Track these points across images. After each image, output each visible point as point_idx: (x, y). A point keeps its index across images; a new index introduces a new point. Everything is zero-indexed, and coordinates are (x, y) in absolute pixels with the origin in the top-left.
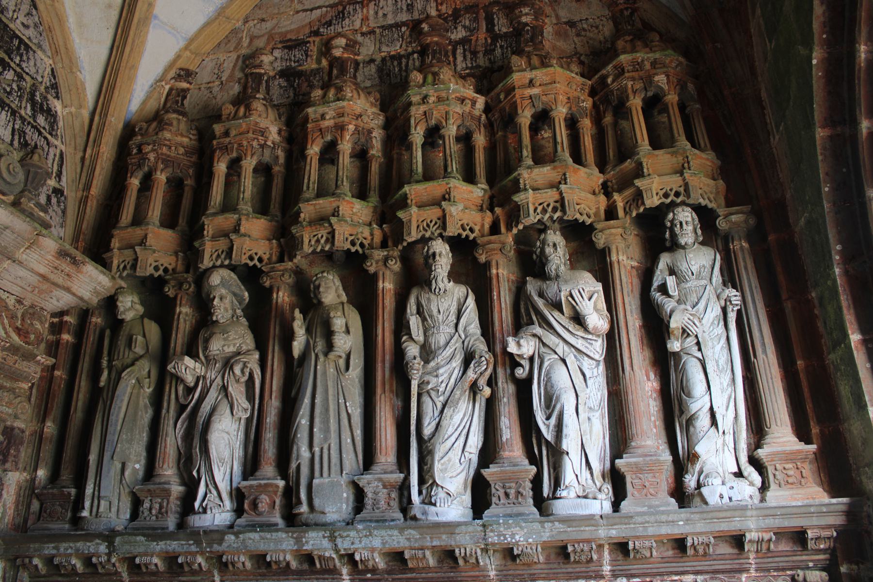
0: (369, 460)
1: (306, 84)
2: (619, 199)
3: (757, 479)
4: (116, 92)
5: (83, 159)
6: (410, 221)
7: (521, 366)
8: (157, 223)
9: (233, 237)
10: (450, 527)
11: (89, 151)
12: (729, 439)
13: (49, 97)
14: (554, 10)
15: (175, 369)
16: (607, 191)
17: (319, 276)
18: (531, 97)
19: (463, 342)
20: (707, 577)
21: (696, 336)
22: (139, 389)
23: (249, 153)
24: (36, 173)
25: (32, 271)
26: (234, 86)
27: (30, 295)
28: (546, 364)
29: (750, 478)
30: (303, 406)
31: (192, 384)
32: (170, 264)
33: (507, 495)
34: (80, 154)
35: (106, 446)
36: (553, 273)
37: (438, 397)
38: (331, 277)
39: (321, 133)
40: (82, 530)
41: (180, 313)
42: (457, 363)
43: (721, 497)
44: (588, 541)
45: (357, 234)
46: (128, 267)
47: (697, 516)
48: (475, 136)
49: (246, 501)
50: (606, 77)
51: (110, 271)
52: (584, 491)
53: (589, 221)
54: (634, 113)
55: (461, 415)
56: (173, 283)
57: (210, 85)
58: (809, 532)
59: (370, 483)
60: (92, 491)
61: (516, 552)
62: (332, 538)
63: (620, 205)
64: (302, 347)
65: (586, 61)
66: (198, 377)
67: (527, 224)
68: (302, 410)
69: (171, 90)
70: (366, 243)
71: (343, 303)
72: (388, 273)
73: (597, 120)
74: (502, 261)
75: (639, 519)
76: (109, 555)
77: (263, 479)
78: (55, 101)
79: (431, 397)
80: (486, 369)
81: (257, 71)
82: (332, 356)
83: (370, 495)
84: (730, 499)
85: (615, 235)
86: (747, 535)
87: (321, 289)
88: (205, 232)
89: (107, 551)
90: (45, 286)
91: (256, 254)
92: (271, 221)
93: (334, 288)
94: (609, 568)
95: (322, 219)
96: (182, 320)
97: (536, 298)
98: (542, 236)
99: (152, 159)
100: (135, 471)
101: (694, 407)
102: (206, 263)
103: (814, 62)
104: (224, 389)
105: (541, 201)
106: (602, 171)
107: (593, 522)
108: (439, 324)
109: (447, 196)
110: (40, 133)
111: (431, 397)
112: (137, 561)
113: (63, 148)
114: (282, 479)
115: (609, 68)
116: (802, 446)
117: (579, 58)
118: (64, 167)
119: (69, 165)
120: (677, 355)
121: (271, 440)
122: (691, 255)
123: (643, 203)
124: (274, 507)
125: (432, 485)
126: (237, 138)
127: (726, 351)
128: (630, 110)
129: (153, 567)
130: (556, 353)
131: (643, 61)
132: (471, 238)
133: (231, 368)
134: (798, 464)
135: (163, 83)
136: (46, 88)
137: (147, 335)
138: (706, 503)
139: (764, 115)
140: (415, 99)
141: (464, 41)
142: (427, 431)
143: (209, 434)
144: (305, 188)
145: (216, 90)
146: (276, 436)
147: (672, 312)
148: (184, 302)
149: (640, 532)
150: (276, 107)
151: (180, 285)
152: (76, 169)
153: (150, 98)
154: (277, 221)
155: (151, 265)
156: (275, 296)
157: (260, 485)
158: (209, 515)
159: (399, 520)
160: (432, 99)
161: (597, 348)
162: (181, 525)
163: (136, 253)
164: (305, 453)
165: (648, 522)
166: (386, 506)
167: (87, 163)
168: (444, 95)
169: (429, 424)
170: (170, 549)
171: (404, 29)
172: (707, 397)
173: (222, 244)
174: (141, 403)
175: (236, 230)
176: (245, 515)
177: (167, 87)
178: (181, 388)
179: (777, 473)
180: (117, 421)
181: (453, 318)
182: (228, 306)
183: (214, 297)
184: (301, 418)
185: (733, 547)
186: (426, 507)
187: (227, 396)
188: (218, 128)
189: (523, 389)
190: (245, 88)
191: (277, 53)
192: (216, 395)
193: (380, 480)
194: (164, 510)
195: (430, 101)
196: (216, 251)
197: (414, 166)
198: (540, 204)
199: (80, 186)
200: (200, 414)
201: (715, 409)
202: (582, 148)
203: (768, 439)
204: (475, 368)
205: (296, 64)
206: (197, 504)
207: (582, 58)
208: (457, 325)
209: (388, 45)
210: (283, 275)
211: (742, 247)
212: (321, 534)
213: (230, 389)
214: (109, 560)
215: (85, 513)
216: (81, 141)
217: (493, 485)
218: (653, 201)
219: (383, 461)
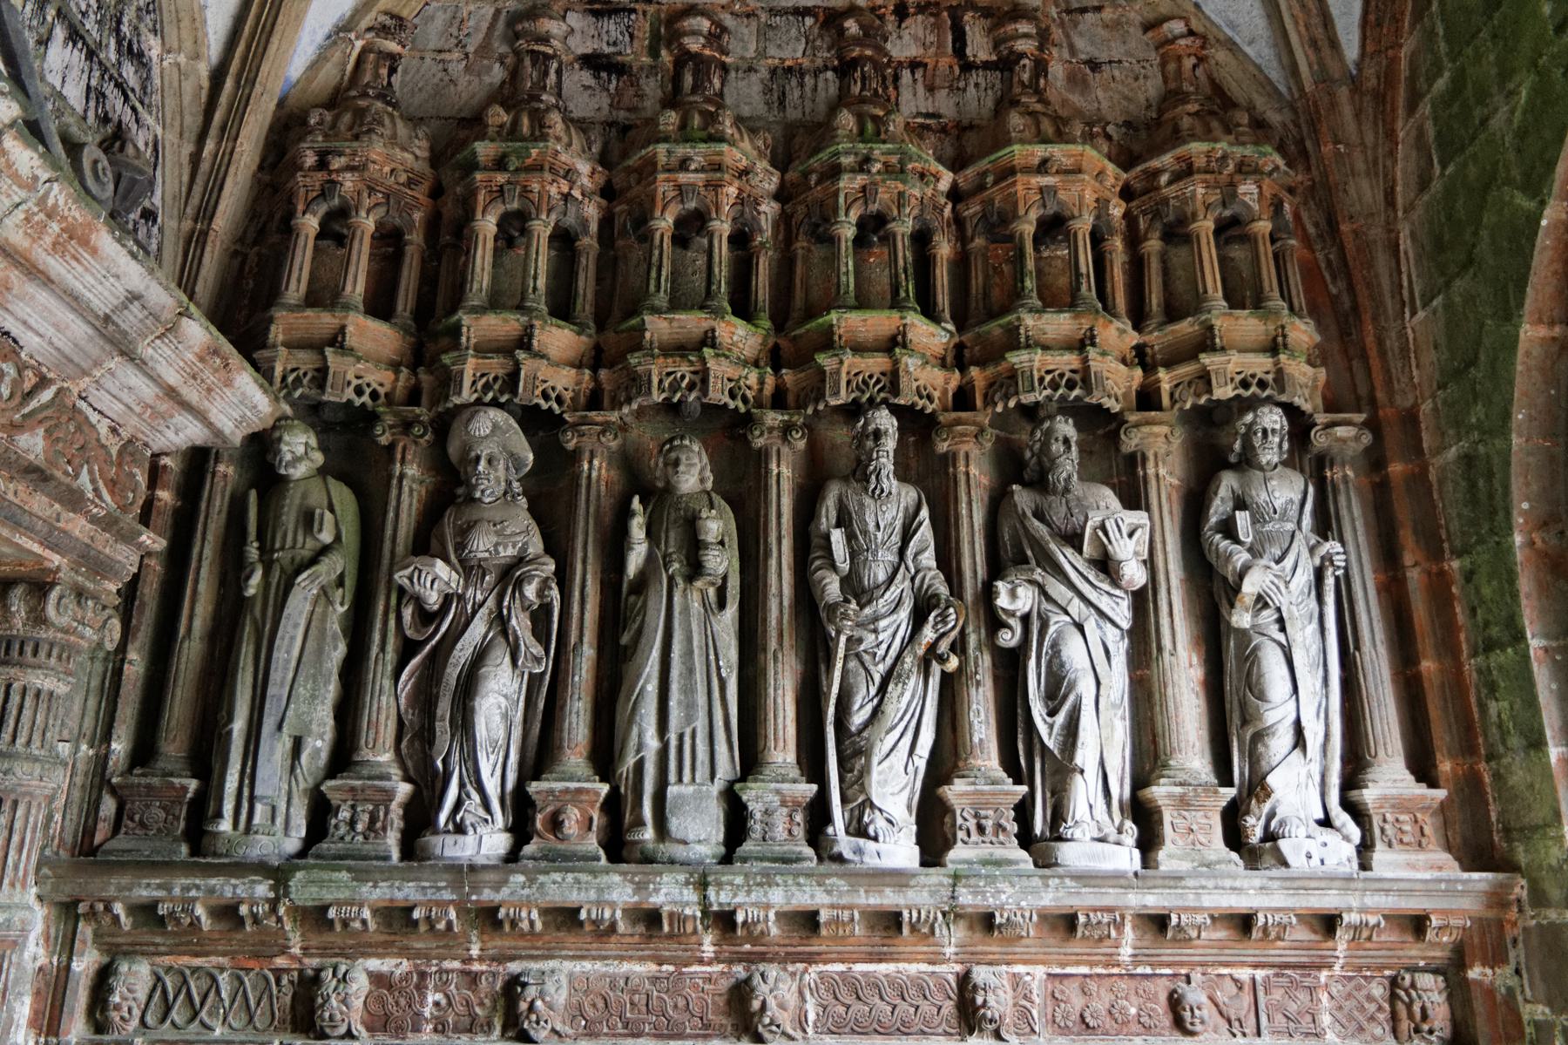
0: (751, 761)
1: (631, 91)
2: (1165, 379)
3: (1355, 833)
4: (275, 40)
5: (195, 159)
6: (838, 372)
7: (1010, 627)
8: (361, 307)
9: (521, 355)
10: (898, 878)
11: (210, 146)
12: (1316, 769)
13: (142, 26)
14: (1068, 36)
15: (411, 579)
16: (1142, 357)
18: (1041, 190)
19: (913, 579)
20: (1271, 972)
21: (1279, 610)
22: (326, 607)
23: (545, 207)
24: (133, 182)
25: (155, 379)
26: (490, 68)
27: (134, 421)
28: (1052, 629)
29: (1344, 831)
31: (436, 607)
32: (381, 385)
33: (981, 829)
34: (188, 148)
35: (267, 706)
36: (1060, 487)
37: (876, 665)
38: (696, 448)
39: (681, 194)
40: (215, 855)
41: (402, 476)
42: (904, 614)
43: (1309, 857)
44: (1110, 910)
45: (738, 381)
46: (305, 381)
47: (1276, 884)
48: (936, 238)
49: (539, 817)
50: (1157, 173)
51: (271, 383)
52: (1100, 829)
53: (1115, 407)
54: (1204, 241)
55: (907, 695)
56: (389, 420)
57: (443, 56)
58: (1433, 917)
59: (756, 796)
60: (236, 784)
61: (998, 920)
62: (702, 885)
63: (1166, 387)
65: (1115, 137)
66: (447, 596)
67: (1024, 401)
69: (365, 51)
70: (749, 394)
71: (708, 493)
72: (785, 450)
73: (1133, 240)
74: (975, 452)
75: (1190, 883)
76: (274, 904)
77: (571, 779)
78: (151, 36)
79: (863, 664)
80: (954, 628)
81: (542, 48)
82: (699, 584)
83: (758, 816)
84: (1322, 862)
85: (1157, 435)
86: (1345, 916)
87: (682, 468)
88: (464, 339)
89: (272, 895)
90: (164, 406)
91: (553, 389)
92: (579, 334)
94: (1130, 951)
95: (679, 349)
96: (406, 489)
97: (1037, 523)
98: (1047, 425)
99: (348, 184)
100: (317, 751)
101: (1270, 717)
102: (467, 395)
103: (1544, 223)
104: (500, 621)
105: (1051, 367)
106: (1138, 326)
107: (1122, 882)
109: (900, 338)
110: (126, 99)
111: (863, 664)
112: (332, 913)
113: (159, 131)
114: (602, 780)
115: (1167, 159)
116: (1421, 790)
117: (1104, 129)
118: (159, 168)
119: (168, 164)
120: (1243, 636)
122: (1274, 483)
123: (1210, 391)
124: (590, 829)
125: (862, 807)
126: (522, 176)
127: (1318, 636)
128: (1198, 237)
129: (357, 925)
130: (1067, 613)
131: (1224, 157)
132: (929, 411)
133: (519, 584)
134: (1419, 816)
135: (352, 36)
136: (139, 9)
137: (337, 508)
138: (1284, 863)
139: (1400, 273)
140: (846, 161)
141: (914, 65)
142: (858, 719)
143: (478, 699)
144: (652, 288)
145: (457, 68)
146: (589, 706)
147: (1246, 569)
148: (409, 457)
149: (1191, 901)
150: (582, 125)
151: (406, 426)
152: (180, 176)
153: (326, 59)
154: (590, 336)
155: (349, 383)
156: (586, 466)
157: (567, 791)
158: (470, 839)
160: (877, 167)
161: (1122, 612)
162: (411, 848)
163: (325, 359)
164: (652, 743)
165: (1203, 887)
166: (785, 835)
167: (205, 166)
168: (894, 159)
169: (862, 707)
170: (399, 895)
171: (809, 21)
172: (1292, 703)
173: (497, 366)
174: (329, 633)
175: (524, 341)
176: (535, 839)
177: (359, 44)
178: (408, 613)
179: (1387, 827)
180: (288, 661)
181: (896, 539)
182: (501, 473)
183: (478, 458)
184: (646, 682)
185: (1315, 932)
186: (861, 841)
187: (504, 632)
188: (484, 150)
189: (1010, 667)
190: (515, 74)
191: (574, 19)
192: (483, 630)
193: (778, 792)
194: (379, 825)
195: (874, 170)
196: (483, 375)
197: (843, 279)
198: (1048, 372)
199: (189, 210)
200: (452, 660)
201: (1304, 723)
202: (1109, 285)
203: (1372, 774)
204: (936, 624)
205: (612, 49)
206: (443, 817)
207: (1110, 129)
208: (902, 552)
209: (779, 46)
210: (603, 432)
211: (1345, 476)
212: (682, 878)
213: (514, 622)
214: (274, 910)
215: (225, 826)
216: (193, 121)
217: (958, 812)
218: (1224, 392)
219: (780, 760)
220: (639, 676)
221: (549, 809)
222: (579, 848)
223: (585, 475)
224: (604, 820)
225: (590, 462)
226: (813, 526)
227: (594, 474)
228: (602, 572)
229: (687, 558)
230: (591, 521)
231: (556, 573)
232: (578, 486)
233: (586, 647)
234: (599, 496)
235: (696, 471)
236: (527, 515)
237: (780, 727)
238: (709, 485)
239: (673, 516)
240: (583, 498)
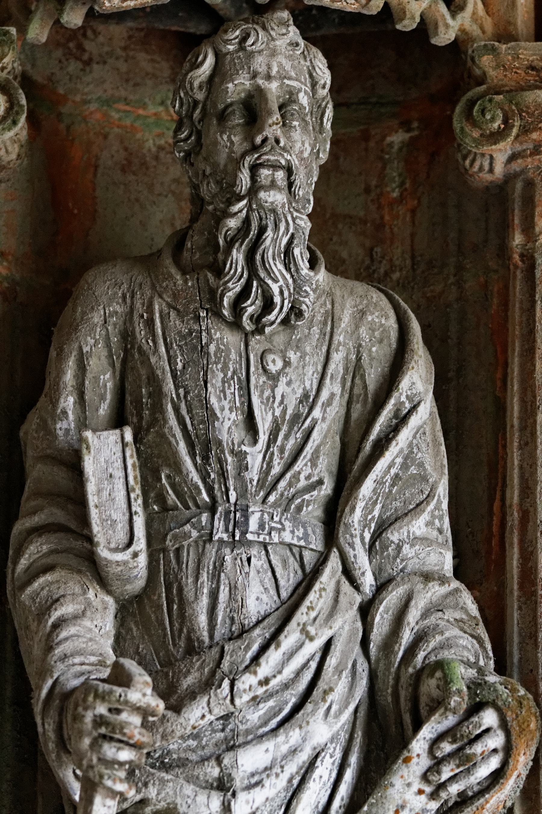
108: (243, 493)
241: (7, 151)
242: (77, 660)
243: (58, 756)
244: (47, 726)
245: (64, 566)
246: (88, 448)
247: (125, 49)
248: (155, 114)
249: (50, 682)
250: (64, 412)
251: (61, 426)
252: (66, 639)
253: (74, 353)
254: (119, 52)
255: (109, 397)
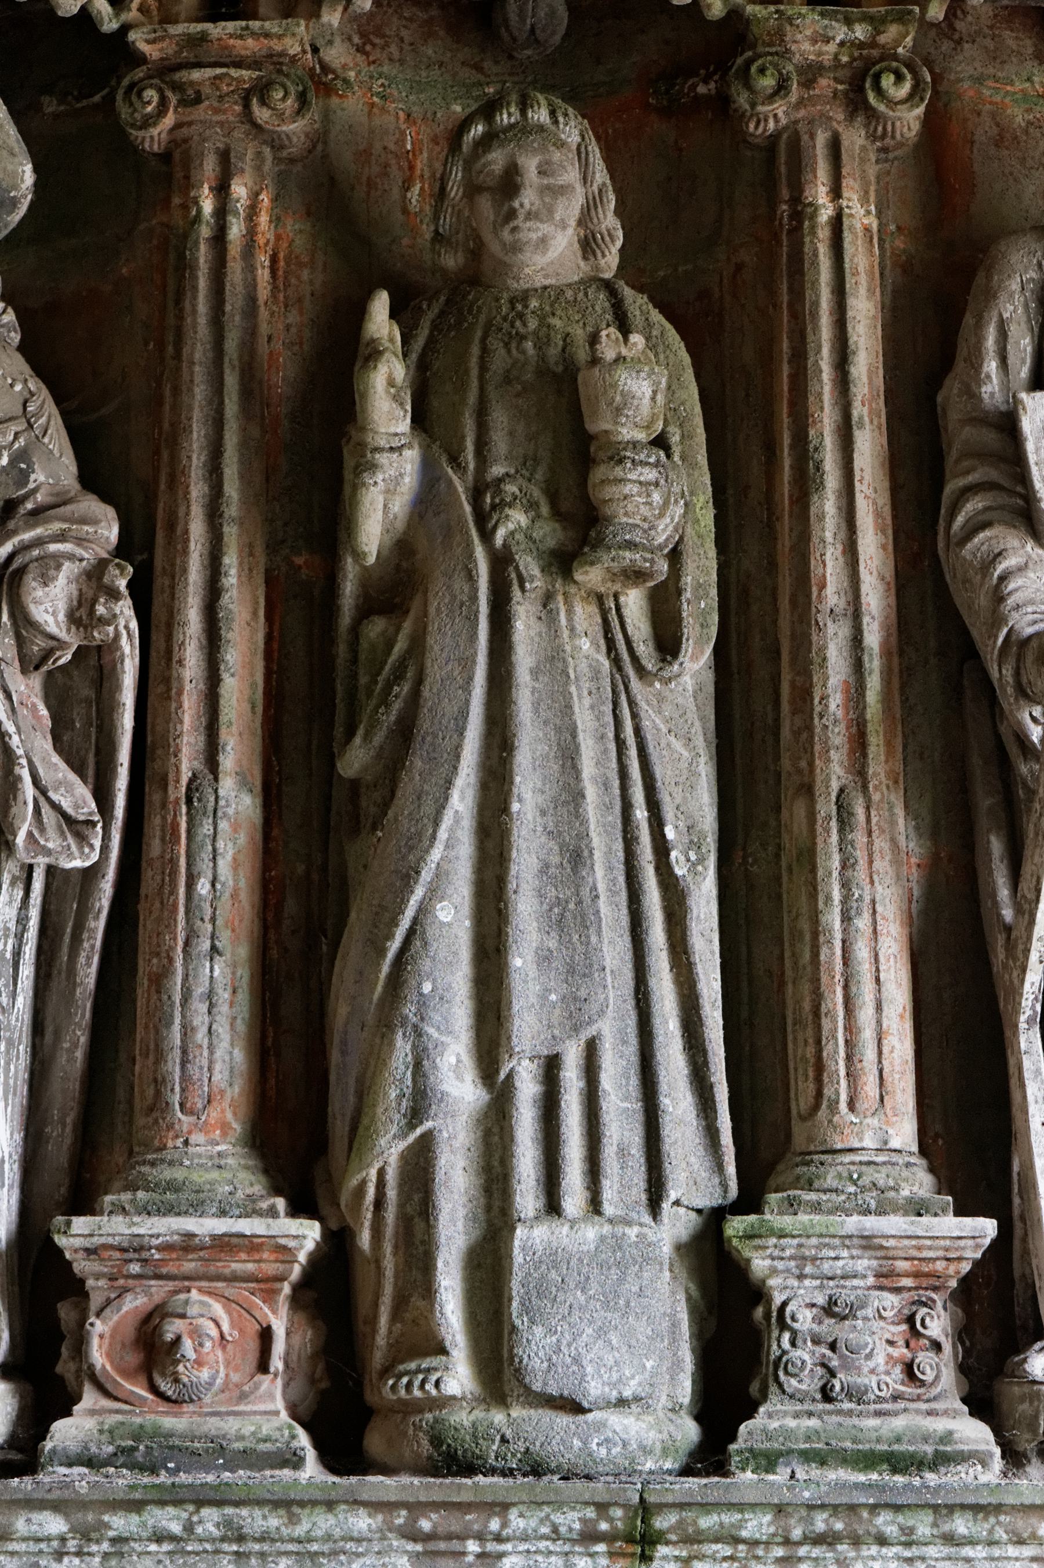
17: (504, 118)
30: (443, 834)
49: (99, 1328)
64: (400, 505)
68: (436, 854)
71: (608, 286)
72: (854, 139)
77: (196, 1208)
83: (805, 1320)
87: (528, 199)
93: (578, 201)
114: (296, 1210)
121: (224, 995)
124: (263, 1366)
146: (244, 973)
156: (208, 206)
157: (187, 1244)
159: (984, 1460)
176: (89, 1398)
184: (433, 893)
193: (868, 1243)
210: (261, 91)
220: (408, 877)
221: (134, 1303)
222: (231, 1426)
223: (205, 231)
224: (306, 1336)
225: (222, 190)
226: (950, 391)
227: (236, 230)
228: (272, 547)
229: (553, 497)
230: (231, 381)
231: (123, 550)
232: (184, 266)
233: (227, 785)
234: (252, 299)
235: (571, 208)
236: (19, 364)
237: (868, 1035)
238: (610, 261)
239: (499, 360)
240: (202, 306)
241: (909, 129)
242: (1030, 610)
243: (1016, 699)
244: (1004, 672)
245: (999, 522)
246: (1024, 409)
247: (991, 27)
248: (1022, 90)
249: (1005, 630)
250: (988, 377)
251: (986, 390)
252: (1016, 590)
253: (995, 319)
254: (986, 31)
255: (1028, 361)
